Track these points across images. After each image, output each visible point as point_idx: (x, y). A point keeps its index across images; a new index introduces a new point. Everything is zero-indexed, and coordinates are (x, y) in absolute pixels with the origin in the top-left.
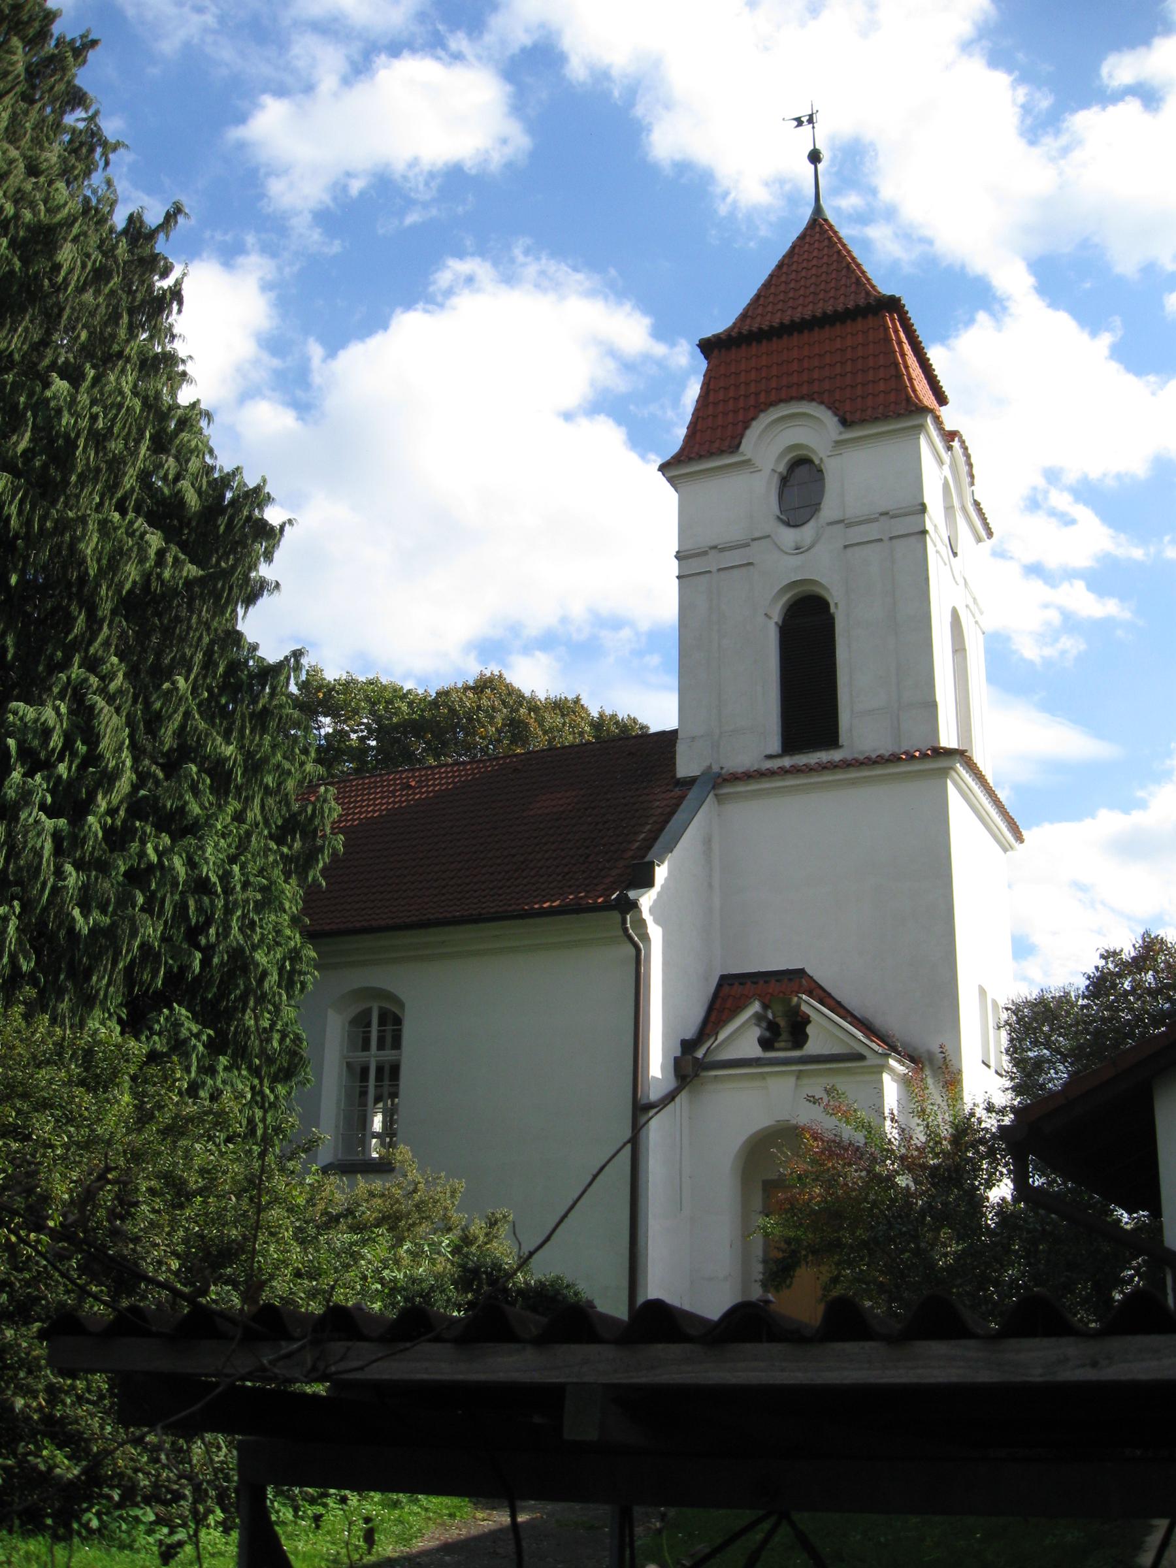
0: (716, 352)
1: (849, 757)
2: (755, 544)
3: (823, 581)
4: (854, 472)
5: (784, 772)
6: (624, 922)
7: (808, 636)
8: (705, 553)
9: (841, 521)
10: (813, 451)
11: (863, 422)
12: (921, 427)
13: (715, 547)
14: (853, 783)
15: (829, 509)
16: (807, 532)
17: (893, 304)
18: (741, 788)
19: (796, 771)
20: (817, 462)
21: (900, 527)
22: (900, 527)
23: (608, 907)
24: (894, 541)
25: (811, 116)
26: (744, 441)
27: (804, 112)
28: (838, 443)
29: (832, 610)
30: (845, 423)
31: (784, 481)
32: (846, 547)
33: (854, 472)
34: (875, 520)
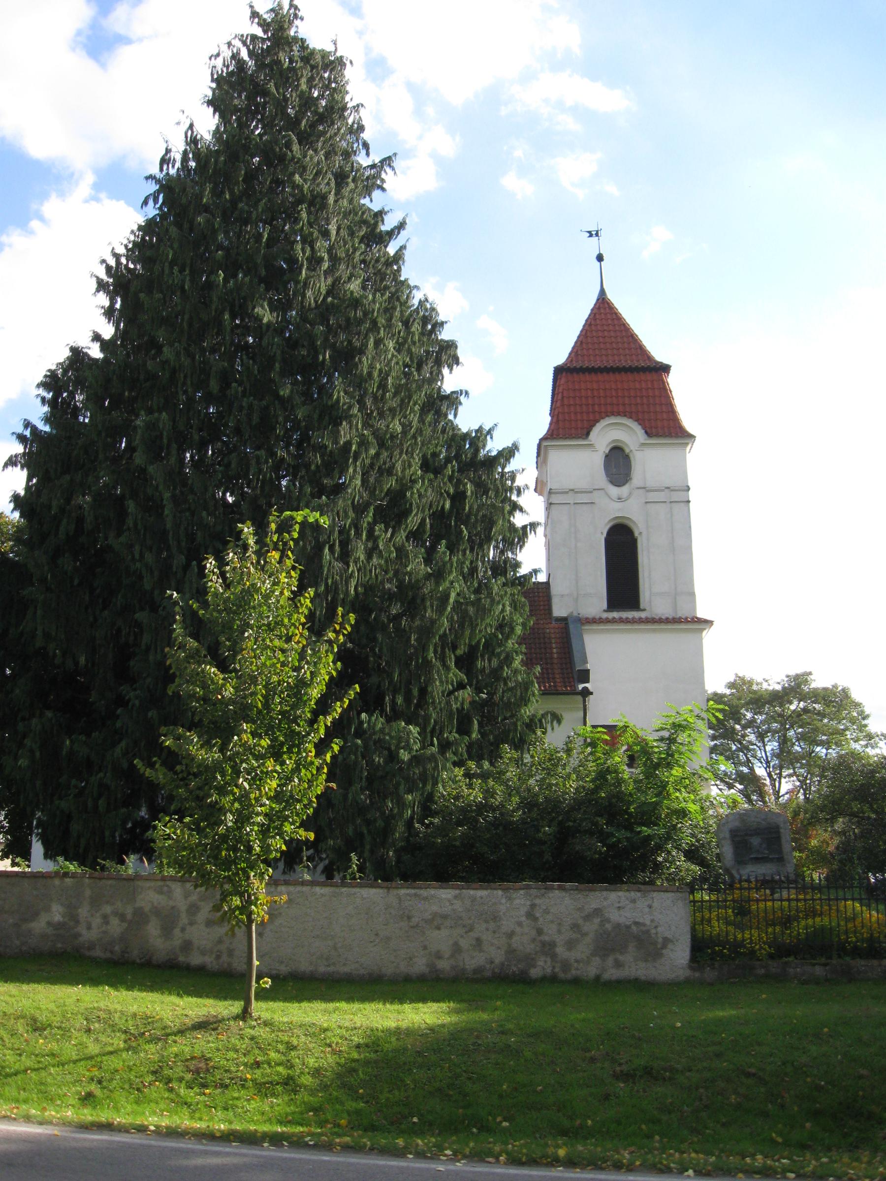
0: (564, 374)
1: (649, 616)
2: (595, 493)
3: (634, 519)
4: (650, 461)
5: (608, 621)
6: (584, 701)
7: (622, 546)
8: (567, 493)
9: (644, 488)
10: (627, 445)
11: (657, 435)
12: (687, 444)
13: (572, 490)
14: (654, 630)
15: (637, 478)
16: (624, 490)
17: (666, 369)
18: (595, 627)
19: (621, 621)
20: (627, 451)
21: (676, 496)
22: (676, 496)
23: (575, 693)
24: (673, 504)
25: (597, 231)
26: (591, 433)
27: (593, 228)
28: (643, 444)
29: (636, 534)
30: (646, 432)
31: (607, 456)
32: (646, 502)
33: (650, 461)
34: (662, 491)
